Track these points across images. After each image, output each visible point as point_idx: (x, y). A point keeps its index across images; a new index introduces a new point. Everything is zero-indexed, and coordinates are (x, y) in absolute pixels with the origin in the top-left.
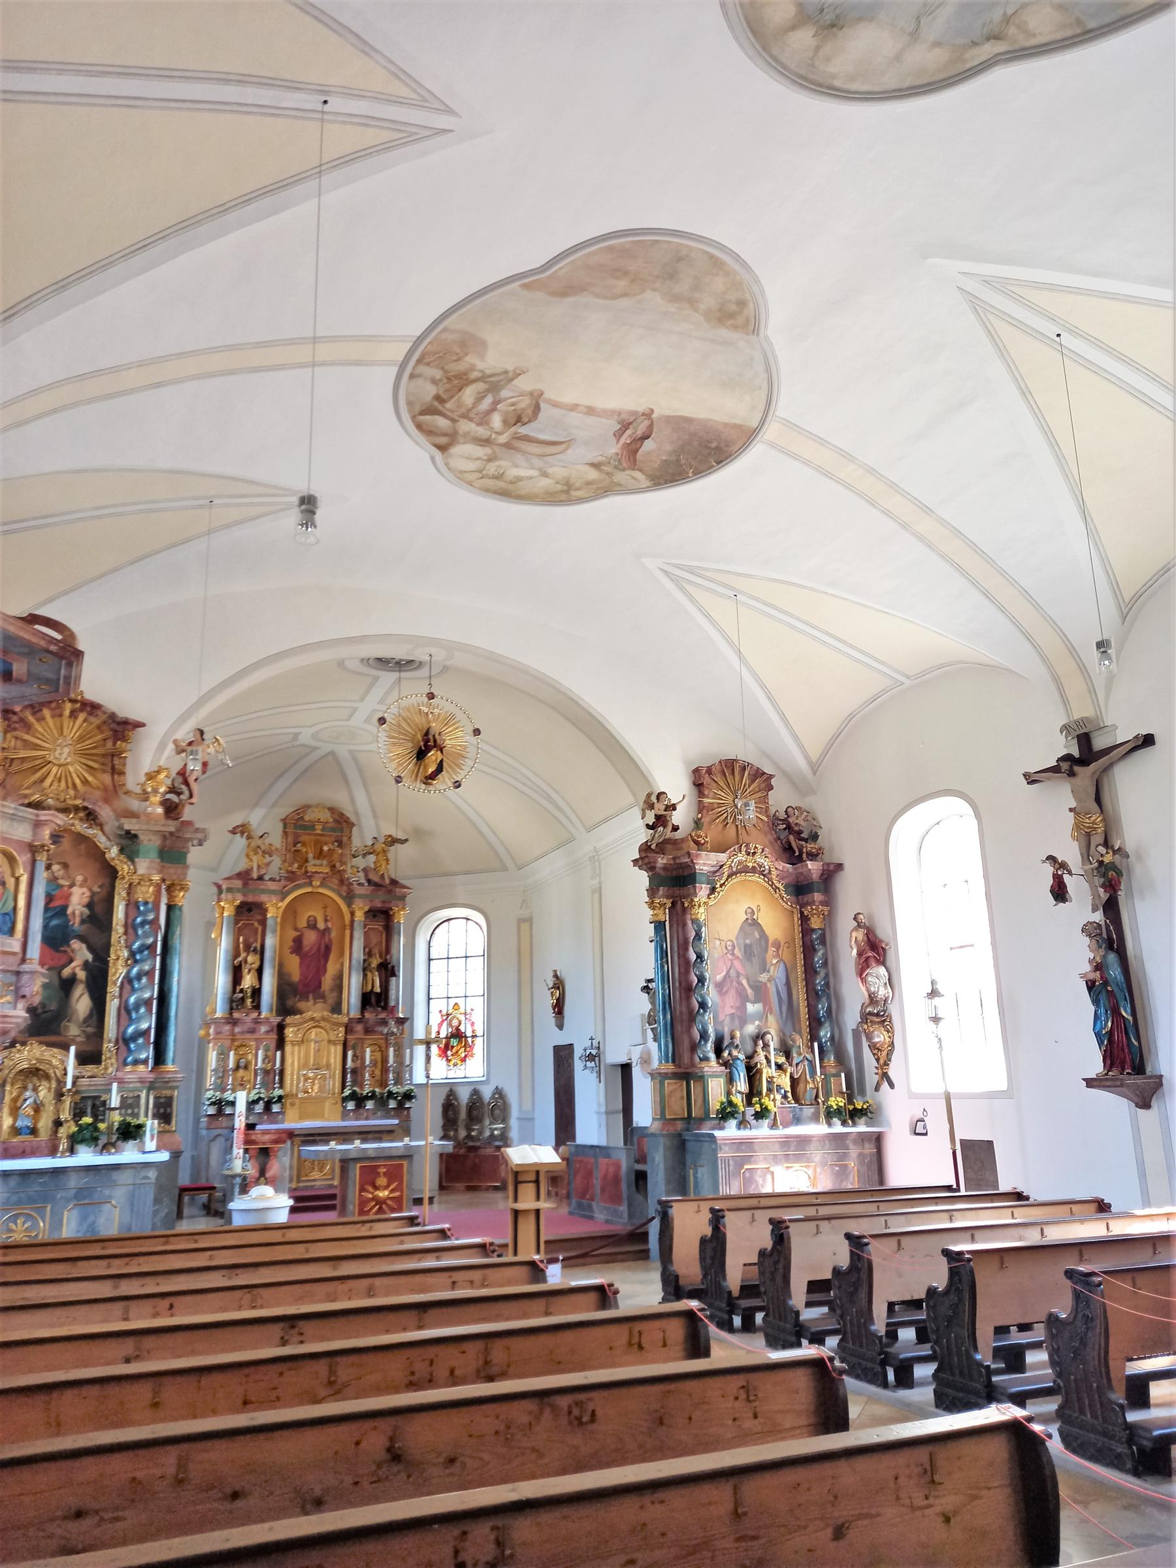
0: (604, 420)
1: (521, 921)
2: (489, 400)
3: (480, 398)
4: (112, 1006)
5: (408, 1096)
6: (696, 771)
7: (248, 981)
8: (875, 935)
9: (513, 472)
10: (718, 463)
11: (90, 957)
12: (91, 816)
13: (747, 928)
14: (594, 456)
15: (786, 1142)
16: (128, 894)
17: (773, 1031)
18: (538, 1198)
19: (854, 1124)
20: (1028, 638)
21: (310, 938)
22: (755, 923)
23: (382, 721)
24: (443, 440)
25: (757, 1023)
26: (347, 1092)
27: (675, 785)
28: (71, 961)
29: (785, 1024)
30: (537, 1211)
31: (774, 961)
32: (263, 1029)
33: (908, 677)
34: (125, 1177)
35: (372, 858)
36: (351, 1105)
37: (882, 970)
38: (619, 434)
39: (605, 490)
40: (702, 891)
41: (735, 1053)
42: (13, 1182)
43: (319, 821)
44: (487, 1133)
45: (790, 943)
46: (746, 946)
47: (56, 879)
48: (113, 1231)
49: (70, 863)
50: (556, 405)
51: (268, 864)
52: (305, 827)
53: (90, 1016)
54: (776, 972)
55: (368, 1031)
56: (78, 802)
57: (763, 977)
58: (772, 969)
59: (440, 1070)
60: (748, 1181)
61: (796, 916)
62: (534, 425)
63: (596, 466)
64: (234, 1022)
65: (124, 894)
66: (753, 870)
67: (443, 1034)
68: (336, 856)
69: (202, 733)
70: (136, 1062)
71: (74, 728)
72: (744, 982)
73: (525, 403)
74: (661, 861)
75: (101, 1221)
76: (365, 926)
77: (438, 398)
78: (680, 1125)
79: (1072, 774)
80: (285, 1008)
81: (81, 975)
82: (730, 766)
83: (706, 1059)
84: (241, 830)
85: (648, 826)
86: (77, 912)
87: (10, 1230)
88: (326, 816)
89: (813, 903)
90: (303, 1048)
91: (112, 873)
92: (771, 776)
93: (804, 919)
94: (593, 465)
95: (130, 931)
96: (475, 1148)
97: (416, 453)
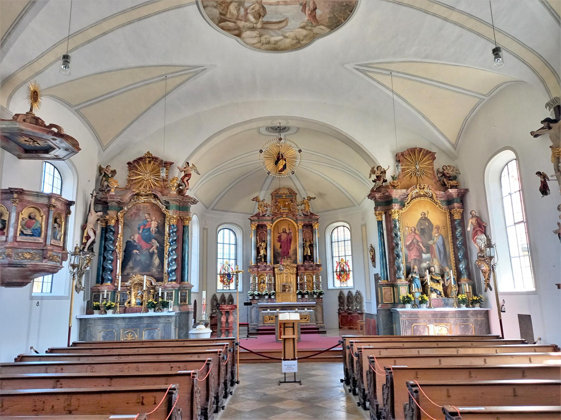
0: (294, 6)
1: (362, 226)
2: (242, 10)
3: (238, 10)
4: (166, 262)
5: (321, 294)
6: (396, 155)
7: (262, 252)
8: (481, 220)
9: (273, 39)
10: (351, 12)
11: (158, 245)
12: (156, 197)
13: (422, 222)
14: (299, 23)
15: (435, 315)
17: (436, 266)
18: (294, 334)
19: (474, 307)
20: (524, 62)
21: (284, 236)
22: (426, 219)
23: (261, 151)
24: (236, 32)
25: (428, 262)
26: (298, 292)
27: (387, 163)
29: (442, 263)
30: (294, 339)
31: (436, 235)
32: (268, 269)
33: (485, 95)
34: (162, 320)
35: (303, 205)
36: (300, 296)
37: (483, 237)
38: (304, 10)
39: (313, 37)
40: (396, 207)
41: (414, 275)
42: (127, 321)
43: (284, 194)
44: (355, 308)
45: (445, 227)
46: (421, 229)
48: (159, 338)
50: (271, 4)
51: (267, 210)
52: (279, 197)
53: (159, 265)
54: (439, 241)
55: (306, 270)
56: (150, 192)
57: (431, 242)
58: (435, 238)
59: (338, 284)
60: (417, 330)
61: (448, 214)
62: (267, 16)
63: (303, 28)
64: (258, 267)
66: (424, 196)
67: (338, 270)
68: (291, 206)
69: (188, 163)
70: (171, 281)
71: (150, 167)
72: (421, 245)
73: (257, 7)
74: (378, 195)
75: (155, 335)
76: (303, 231)
77: (221, 14)
78: (390, 306)
79: (550, 128)
80: (276, 262)
81: (156, 251)
82: (413, 151)
83: (400, 278)
84: (256, 199)
85: (373, 181)
87: (127, 337)
88: (286, 192)
89: (454, 208)
90: (281, 276)
91: (164, 216)
92: (435, 153)
93: (451, 215)
94: (301, 28)
96: (351, 313)
97: (229, 40)
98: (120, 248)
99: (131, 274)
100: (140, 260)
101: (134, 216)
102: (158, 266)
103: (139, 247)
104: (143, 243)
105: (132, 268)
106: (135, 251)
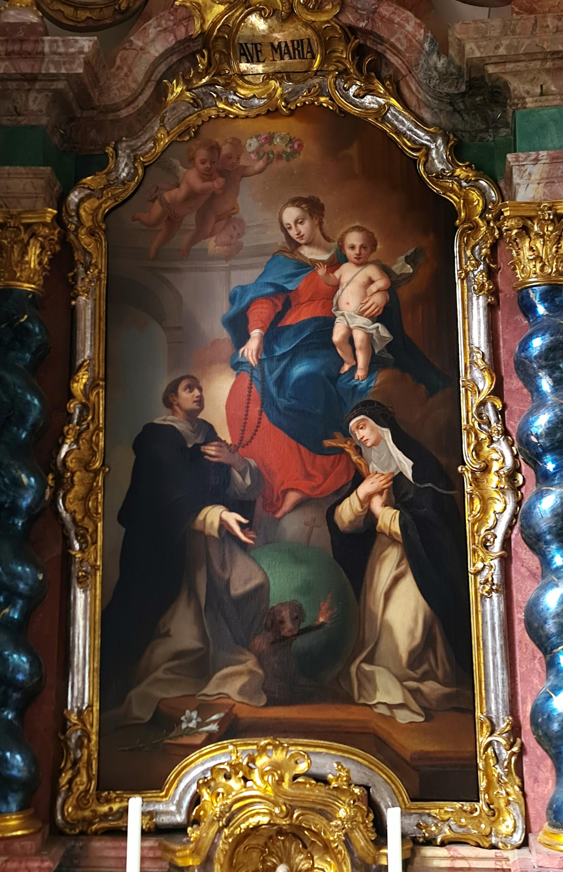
11: (406, 466)
16: (491, 274)
28: (358, 479)
47: (294, 245)
49: (328, 200)
65: (479, 275)
81: (389, 519)
86: (359, 336)
95: (513, 383)
98: (90, 490)
99: (191, 719)
100: (262, 590)
101: (190, 220)
102: (417, 657)
103: (242, 481)
104: (275, 451)
105: (200, 666)
106: (214, 516)
